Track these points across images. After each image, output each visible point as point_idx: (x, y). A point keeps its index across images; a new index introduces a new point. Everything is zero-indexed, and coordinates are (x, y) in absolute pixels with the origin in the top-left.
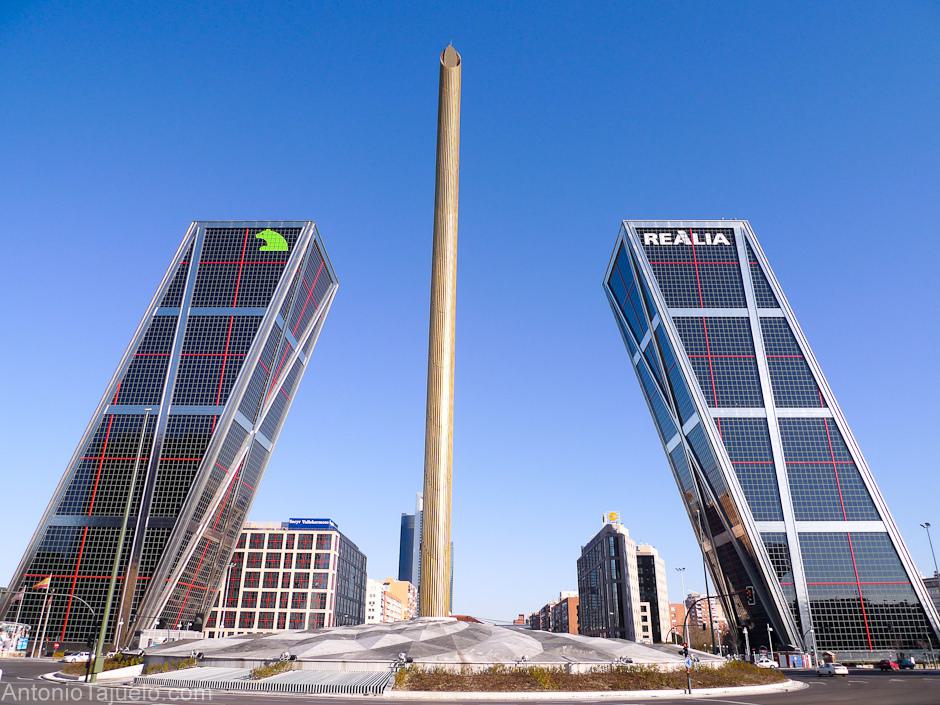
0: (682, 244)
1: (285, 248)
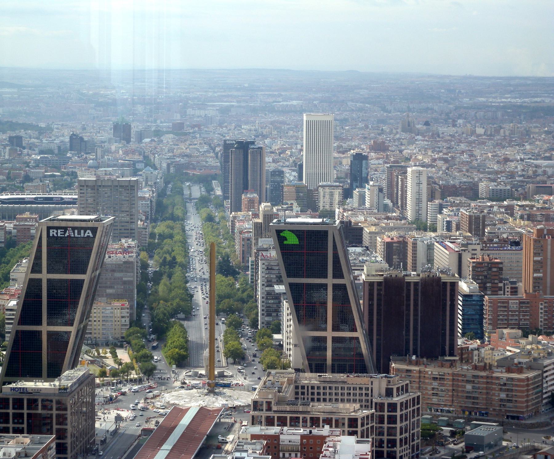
0: (69, 236)
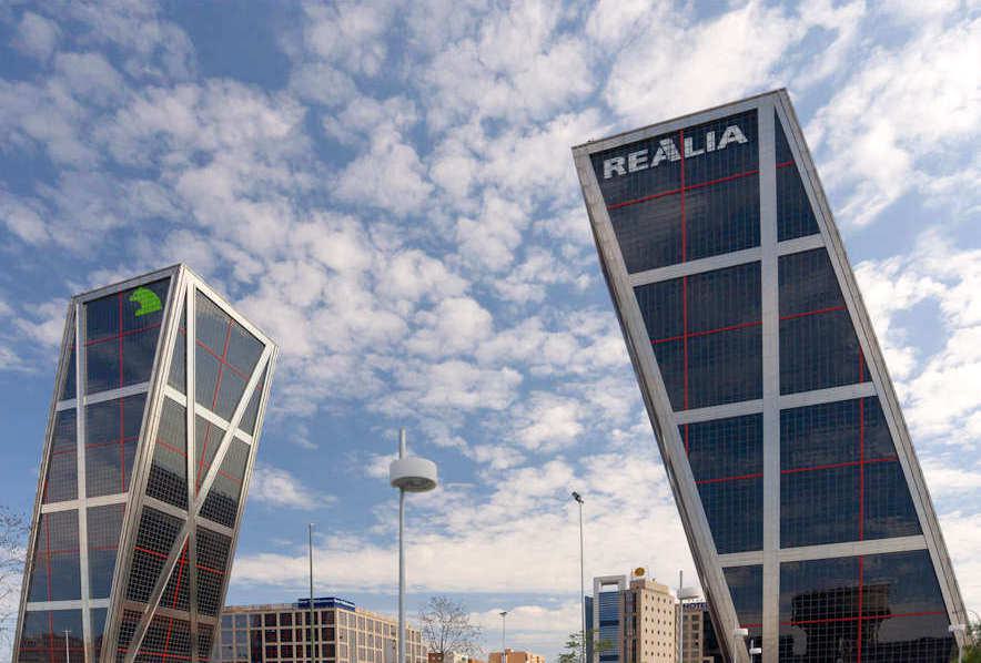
1: (158, 308)
